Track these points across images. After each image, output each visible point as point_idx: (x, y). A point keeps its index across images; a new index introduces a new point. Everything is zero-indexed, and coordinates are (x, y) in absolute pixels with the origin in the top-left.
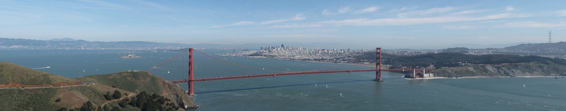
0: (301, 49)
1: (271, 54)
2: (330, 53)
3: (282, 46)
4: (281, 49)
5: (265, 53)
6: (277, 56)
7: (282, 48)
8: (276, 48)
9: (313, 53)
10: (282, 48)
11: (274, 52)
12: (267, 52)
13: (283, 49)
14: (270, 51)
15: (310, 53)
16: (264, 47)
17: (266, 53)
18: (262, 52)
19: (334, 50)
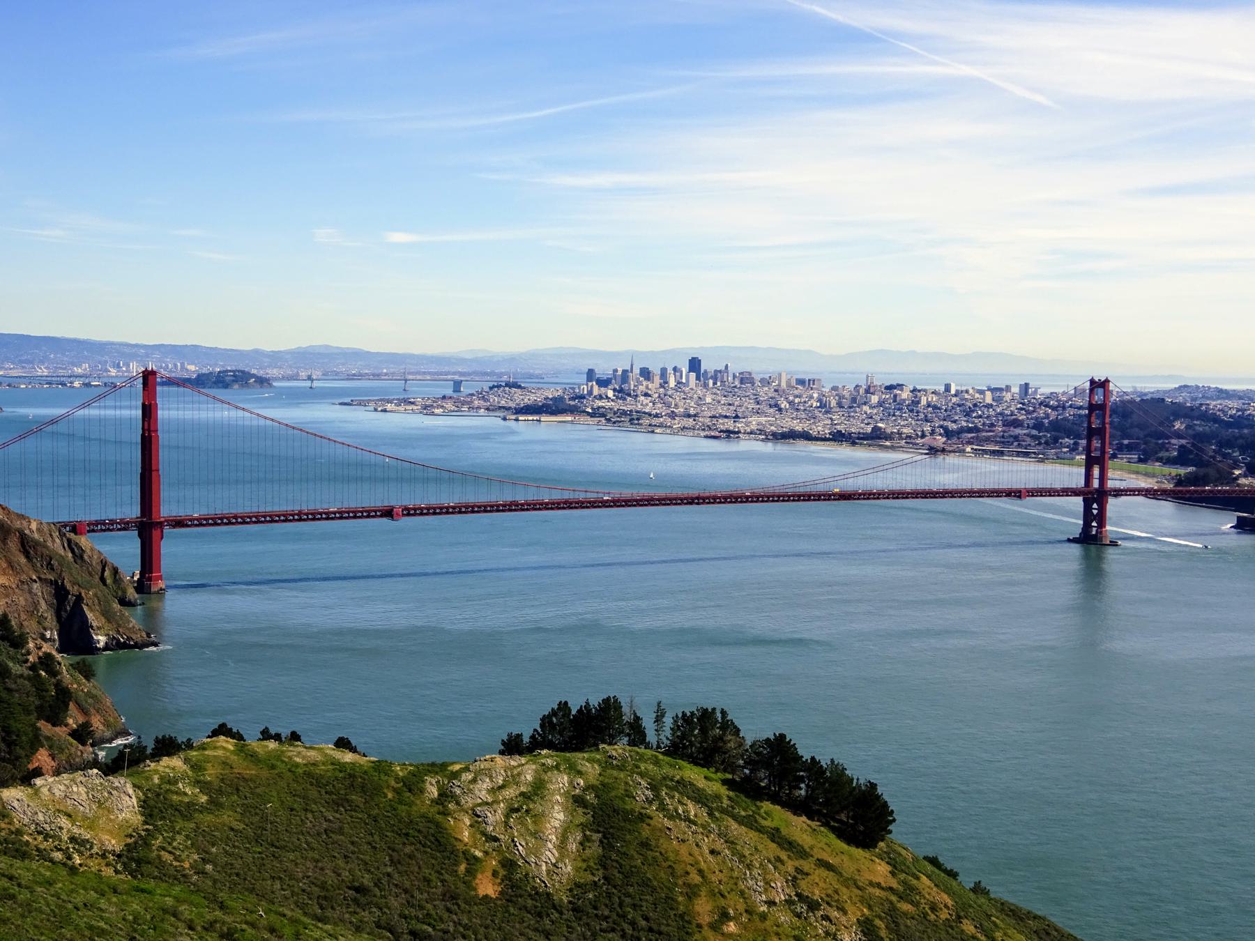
0: (784, 385)
1: (629, 405)
2: (924, 402)
3: (695, 364)
4: (686, 384)
5: (600, 397)
6: (657, 416)
7: (693, 375)
8: (657, 380)
9: (840, 405)
10: (693, 375)
11: (646, 395)
12: (610, 394)
13: (698, 378)
14: (622, 393)
15: (823, 405)
16: (603, 370)
17: (607, 398)
18: (582, 397)
19: (948, 388)
